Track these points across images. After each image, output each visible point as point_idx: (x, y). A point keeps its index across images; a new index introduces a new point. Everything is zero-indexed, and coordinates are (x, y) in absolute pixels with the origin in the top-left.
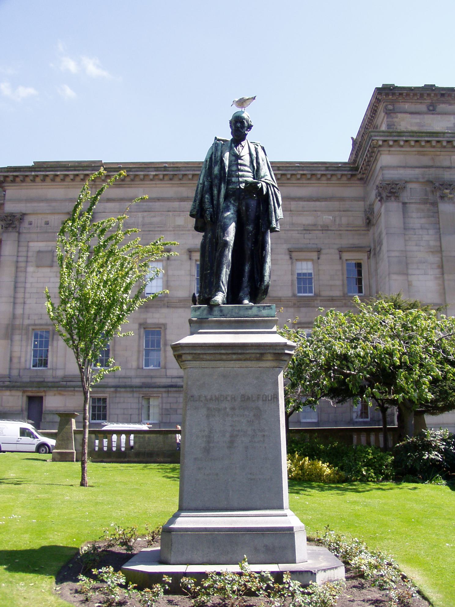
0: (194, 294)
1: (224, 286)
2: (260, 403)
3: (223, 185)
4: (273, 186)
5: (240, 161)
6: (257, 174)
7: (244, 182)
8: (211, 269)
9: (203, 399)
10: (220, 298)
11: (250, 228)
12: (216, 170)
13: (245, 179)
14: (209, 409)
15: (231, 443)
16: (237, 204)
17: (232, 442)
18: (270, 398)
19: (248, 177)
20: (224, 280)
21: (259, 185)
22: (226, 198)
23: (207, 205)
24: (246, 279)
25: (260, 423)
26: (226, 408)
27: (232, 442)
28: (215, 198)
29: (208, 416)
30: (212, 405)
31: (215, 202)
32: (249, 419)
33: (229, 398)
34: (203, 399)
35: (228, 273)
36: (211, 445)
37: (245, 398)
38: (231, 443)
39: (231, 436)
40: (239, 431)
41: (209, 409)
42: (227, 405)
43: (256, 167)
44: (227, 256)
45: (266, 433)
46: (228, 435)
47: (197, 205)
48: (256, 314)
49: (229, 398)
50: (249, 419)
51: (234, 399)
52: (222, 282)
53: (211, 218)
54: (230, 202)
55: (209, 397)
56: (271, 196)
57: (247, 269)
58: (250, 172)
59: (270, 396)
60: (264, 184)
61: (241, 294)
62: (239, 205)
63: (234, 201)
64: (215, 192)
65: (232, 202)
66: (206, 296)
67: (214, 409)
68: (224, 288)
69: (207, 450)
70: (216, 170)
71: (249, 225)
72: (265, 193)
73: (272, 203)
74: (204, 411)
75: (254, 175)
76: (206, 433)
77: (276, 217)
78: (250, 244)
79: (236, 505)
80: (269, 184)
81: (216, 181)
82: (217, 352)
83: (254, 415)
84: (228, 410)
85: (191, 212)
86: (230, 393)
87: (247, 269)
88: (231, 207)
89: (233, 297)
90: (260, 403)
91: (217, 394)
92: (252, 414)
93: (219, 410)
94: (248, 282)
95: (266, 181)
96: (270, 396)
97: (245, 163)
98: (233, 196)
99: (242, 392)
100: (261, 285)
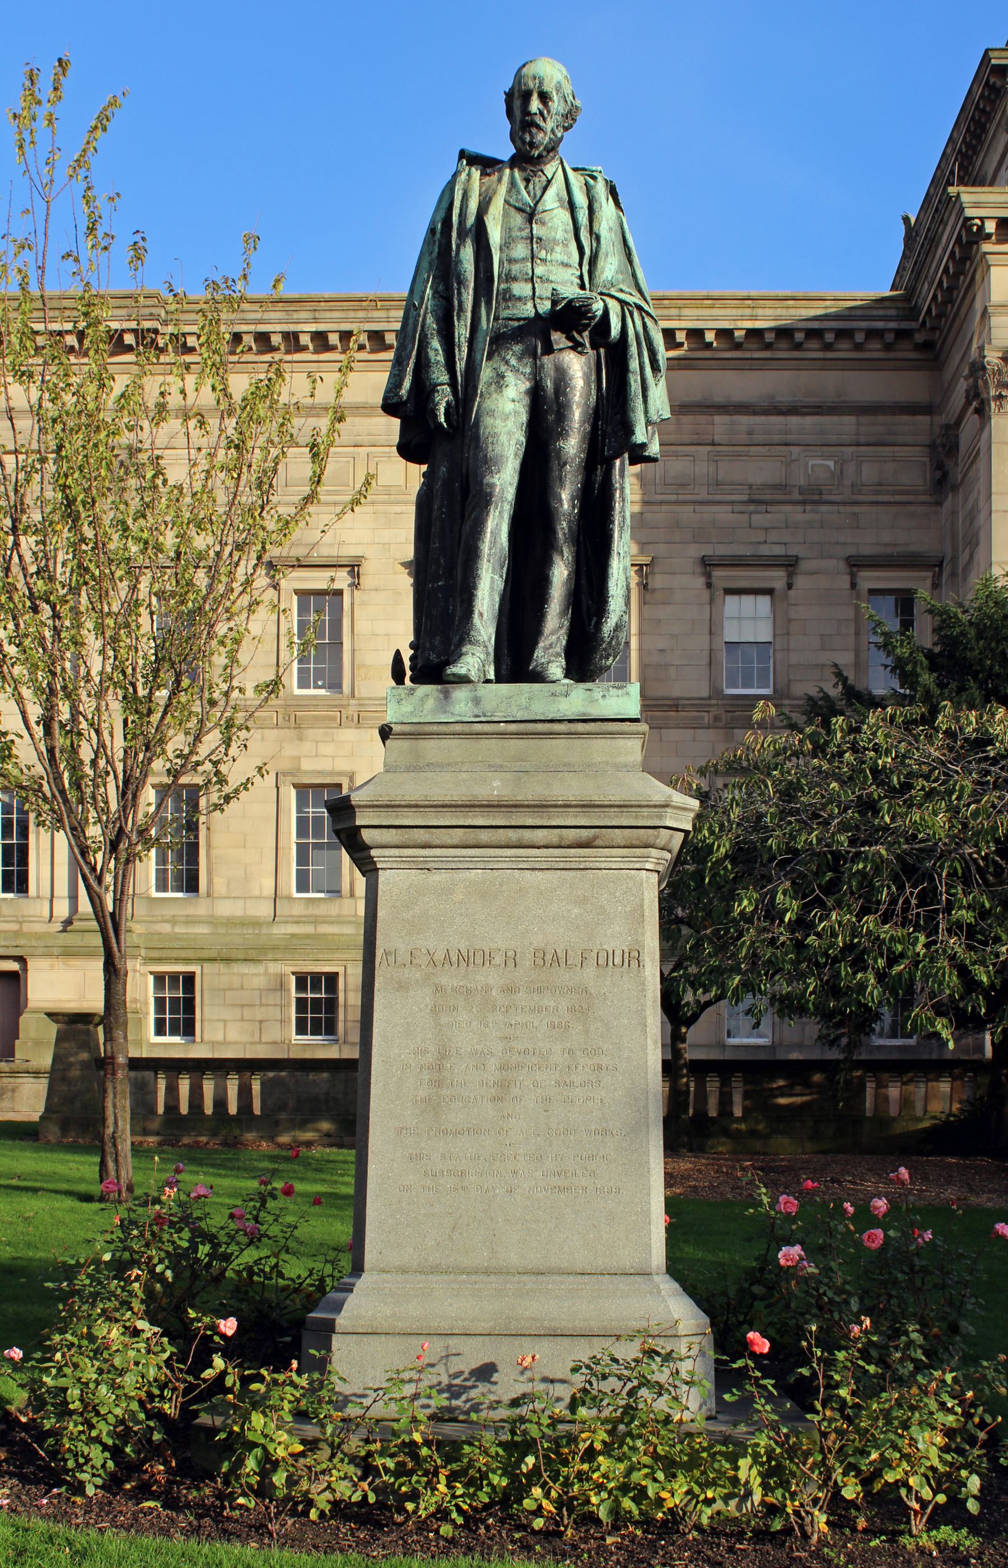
0: (398, 653)
2: (590, 970)
4: (640, 308)
6: (590, 273)
16: (528, 370)
17: (504, 1085)
18: (618, 960)
21: (598, 307)
25: (587, 1032)
26: (487, 989)
27: (504, 1085)
29: (435, 1010)
30: (448, 979)
31: (460, 366)
33: (498, 960)
34: (423, 960)
35: (500, 585)
36: (445, 1092)
37: (549, 960)
39: (502, 1068)
41: (438, 989)
42: (490, 977)
45: (605, 1061)
46: (492, 1063)
48: (582, 710)
49: (498, 960)
51: (512, 960)
52: (481, 615)
54: (507, 363)
55: (440, 956)
56: (633, 349)
58: (567, 265)
60: (614, 308)
61: (539, 653)
63: (520, 359)
65: (513, 362)
66: (433, 657)
67: (454, 990)
73: (634, 365)
75: (581, 277)
76: (430, 1058)
83: (572, 1010)
85: (385, 399)
88: (510, 378)
89: (515, 663)
90: (590, 970)
92: (564, 1004)
94: (563, 613)
99: (537, 940)
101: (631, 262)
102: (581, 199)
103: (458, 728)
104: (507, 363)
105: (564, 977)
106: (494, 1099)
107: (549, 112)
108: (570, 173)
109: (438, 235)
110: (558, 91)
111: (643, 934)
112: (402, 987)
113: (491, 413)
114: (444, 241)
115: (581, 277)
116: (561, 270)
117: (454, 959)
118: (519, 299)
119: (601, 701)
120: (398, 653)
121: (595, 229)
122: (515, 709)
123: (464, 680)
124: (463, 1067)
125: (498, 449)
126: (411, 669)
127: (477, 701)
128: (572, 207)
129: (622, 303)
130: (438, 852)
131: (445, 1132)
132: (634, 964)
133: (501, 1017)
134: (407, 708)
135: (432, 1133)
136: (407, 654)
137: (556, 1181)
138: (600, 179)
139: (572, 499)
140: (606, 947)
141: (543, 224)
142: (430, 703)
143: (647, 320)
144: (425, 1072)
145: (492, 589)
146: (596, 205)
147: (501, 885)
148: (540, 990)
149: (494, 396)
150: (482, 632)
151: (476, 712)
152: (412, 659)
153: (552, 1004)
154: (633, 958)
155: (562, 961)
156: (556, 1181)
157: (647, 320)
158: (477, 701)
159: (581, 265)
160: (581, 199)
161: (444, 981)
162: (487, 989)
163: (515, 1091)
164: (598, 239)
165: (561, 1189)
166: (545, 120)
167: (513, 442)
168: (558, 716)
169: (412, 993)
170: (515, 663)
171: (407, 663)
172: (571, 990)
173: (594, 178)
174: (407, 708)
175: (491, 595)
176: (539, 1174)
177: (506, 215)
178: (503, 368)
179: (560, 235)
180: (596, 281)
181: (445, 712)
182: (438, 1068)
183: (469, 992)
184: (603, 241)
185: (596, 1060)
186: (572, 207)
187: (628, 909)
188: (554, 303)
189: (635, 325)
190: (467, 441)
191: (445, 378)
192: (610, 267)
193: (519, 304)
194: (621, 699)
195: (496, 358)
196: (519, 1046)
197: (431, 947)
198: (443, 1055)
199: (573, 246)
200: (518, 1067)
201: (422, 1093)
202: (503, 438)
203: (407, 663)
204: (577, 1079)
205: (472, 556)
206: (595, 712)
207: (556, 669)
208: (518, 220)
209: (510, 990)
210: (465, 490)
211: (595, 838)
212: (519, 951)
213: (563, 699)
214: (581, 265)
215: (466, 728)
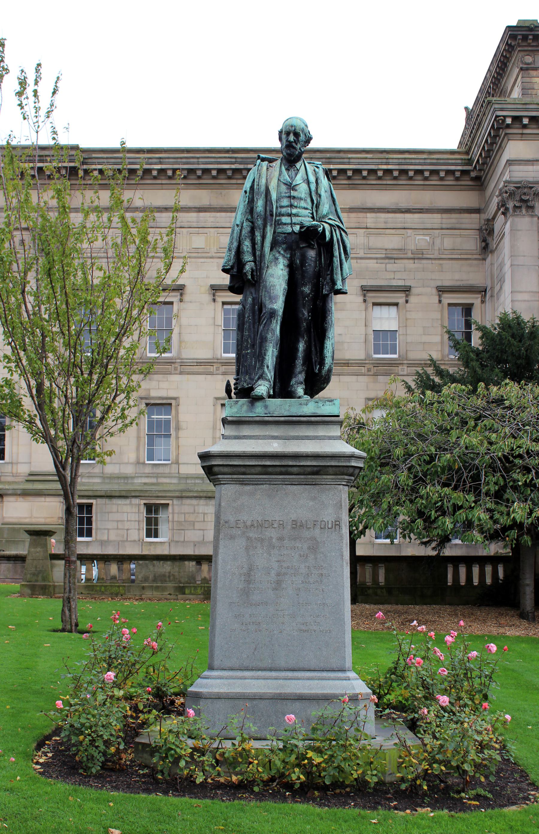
0: (228, 381)
1: (270, 372)
2: (317, 531)
3: (269, 228)
4: (339, 227)
5: (293, 193)
6: (317, 211)
7: (298, 224)
8: (253, 346)
9: (241, 525)
10: (262, 388)
11: (307, 290)
12: (260, 205)
13: (300, 219)
16: (289, 256)
17: (279, 583)
18: (330, 526)
19: (304, 217)
20: (269, 364)
21: (320, 229)
22: (274, 245)
23: (248, 257)
24: (299, 362)
25: (316, 558)
27: (279, 583)
28: (258, 247)
29: (247, 549)
31: (258, 253)
32: (302, 553)
34: (241, 525)
35: (276, 353)
36: (251, 586)
37: (297, 525)
38: (278, 585)
39: (278, 575)
41: (248, 538)
42: (272, 533)
43: (315, 202)
44: (273, 331)
45: (324, 572)
46: (273, 573)
47: (232, 257)
48: (313, 411)
49: (276, 525)
50: (302, 553)
51: (282, 525)
52: (268, 367)
53: (252, 275)
54: (279, 252)
55: (249, 523)
56: (336, 246)
57: (301, 346)
58: (306, 209)
59: (330, 522)
60: (327, 227)
61: (293, 382)
62: (291, 257)
63: (285, 251)
64: (258, 238)
65: (282, 252)
66: (245, 385)
67: (255, 539)
68: (270, 374)
69: (246, 593)
70: (260, 205)
71: (305, 285)
72: (327, 239)
73: (336, 253)
74: (242, 542)
76: (245, 571)
77: (342, 275)
78: (306, 313)
79: (282, 664)
80: (333, 226)
81: (260, 222)
82: (260, 463)
83: (309, 548)
84: (274, 540)
86: (277, 519)
87: (301, 346)
90: (317, 531)
91: (259, 519)
92: (305, 546)
93: (262, 540)
94: (303, 365)
95: (330, 222)
96: (330, 522)
97: (299, 196)
98: (284, 243)
99: (293, 517)
100: (320, 370)
101: (335, 204)
102: (312, 179)
103: (258, 419)
104: (279, 252)
105: (307, 534)
107: (298, 141)
108: (307, 164)
109: (248, 194)
110: (302, 132)
111: (342, 514)
113: (272, 276)
114: (251, 196)
115: (312, 214)
116: (304, 211)
118: (285, 224)
119: (322, 407)
120: (228, 381)
121: (319, 192)
122: (283, 411)
123: (260, 398)
125: (275, 292)
126: (235, 389)
127: (266, 407)
128: (308, 183)
129: (330, 225)
130: (249, 476)
134: (234, 410)
136: (232, 382)
138: (321, 168)
139: (308, 313)
141: (296, 190)
142: (245, 408)
143: (342, 232)
145: (273, 355)
146: (319, 181)
148: (295, 539)
149: (274, 267)
150: (268, 374)
151: (266, 412)
152: (234, 385)
155: (305, 526)
157: (342, 232)
158: (266, 407)
159: (312, 208)
160: (312, 179)
161: (251, 535)
163: (284, 586)
164: (320, 196)
166: (297, 144)
167: (282, 289)
168: (303, 414)
169: (236, 540)
170: (282, 390)
171: (233, 387)
173: (318, 167)
174: (234, 410)
175: (272, 358)
177: (278, 186)
178: (277, 255)
179: (303, 196)
180: (319, 212)
181: (252, 412)
182: (248, 576)
183: (262, 540)
184: (322, 197)
185: (320, 572)
186: (308, 183)
188: (301, 228)
189: (336, 236)
190: (261, 288)
191: (251, 258)
192: (325, 207)
193: (285, 226)
194: (331, 407)
195: (274, 250)
196: (285, 565)
197: (245, 519)
198: (250, 569)
199: (309, 200)
200: (285, 574)
202: (278, 287)
203: (233, 387)
204: (311, 580)
205: (264, 340)
206: (320, 412)
207: (300, 390)
208: (283, 188)
209: (281, 539)
210: (260, 310)
211: (320, 471)
213: (305, 406)
214: (312, 208)
215: (261, 419)
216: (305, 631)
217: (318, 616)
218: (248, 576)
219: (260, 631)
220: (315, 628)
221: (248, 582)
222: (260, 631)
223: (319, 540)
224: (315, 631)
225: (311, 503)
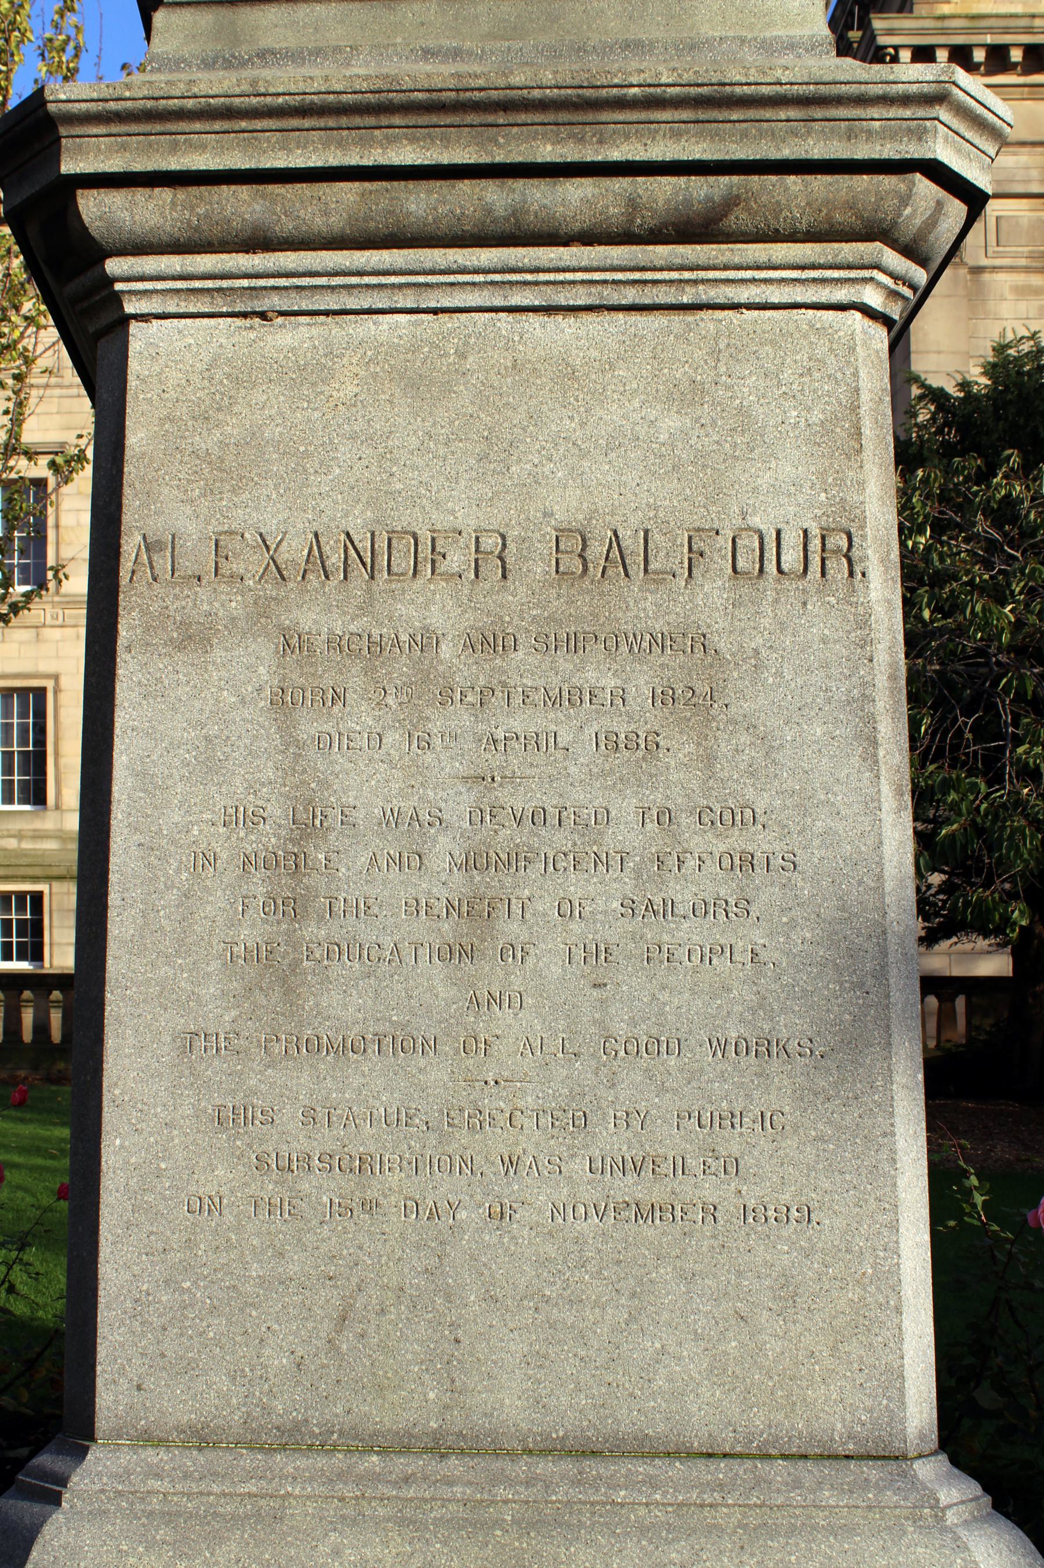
2: (714, 589)
14: (292, 643)
15: (474, 926)
17: (478, 911)
18: (791, 558)
25: (709, 759)
27: (478, 911)
29: (283, 703)
30: (316, 615)
33: (456, 560)
34: (249, 563)
36: (312, 931)
37: (593, 558)
38: (474, 926)
40: (539, 817)
41: (292, 643)
42: (434, 608)
45: (762, 843)
46: (444, 848)
49: (456, 560)
51: (494, 560)
55: (294, 551)
59: (792, 540)
67: (335, 643)
69: (277, 971)
74: (250, 665)
76: (268, 838)
83: (664, 697)
84: (446, 651)
86: (468, 519)
90: (714, 589)
91: (358, 523)
92: (642, 683)
96: (792, 540)
99: (566, 505)
105: (643, 608)
106: (457, 953)
111: (861, 485)
112: (193, 637)
117: (335, 559)
124: (364, 860)
130: (289, 260)
131: (315, 1047)
132: (838, 568)
133: (467, 720)
135: (278, 1049)
137: (627, 1187)
140: (756, 521)
144: (258, 876)
147: (462, 356)
148: (574, 644)
153: (610, 682)
154: (833, 551)
156: (627, 1187)
162: (426, 641)
163: (512, 929)
165: (644, 1212)
169: (218, 654)
172: (661, 642)
176: (579, 1166)
182: (292, 866)
183: (376, 647)
185: (736, 841)
187: (816, 416)
196: (520, 801)
197: (271, 526)
198: (307, 825)
200: (516, 860)
201: (250, 933)
209: (489, 642)
211: (731, 202)
212: (512, 534)
216: (644, 1212)
217: (734, 1119)
218: (292, 866)
219: (370, 1206)
220: (709, 1190)
221: (293, 908)
222: (370, 1206)
223: (723, 644)
224: (711, 1211)
225: (671, 423)
